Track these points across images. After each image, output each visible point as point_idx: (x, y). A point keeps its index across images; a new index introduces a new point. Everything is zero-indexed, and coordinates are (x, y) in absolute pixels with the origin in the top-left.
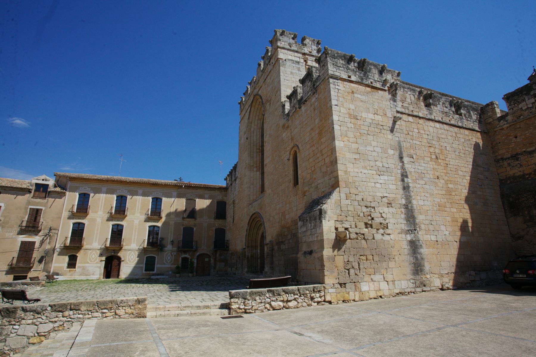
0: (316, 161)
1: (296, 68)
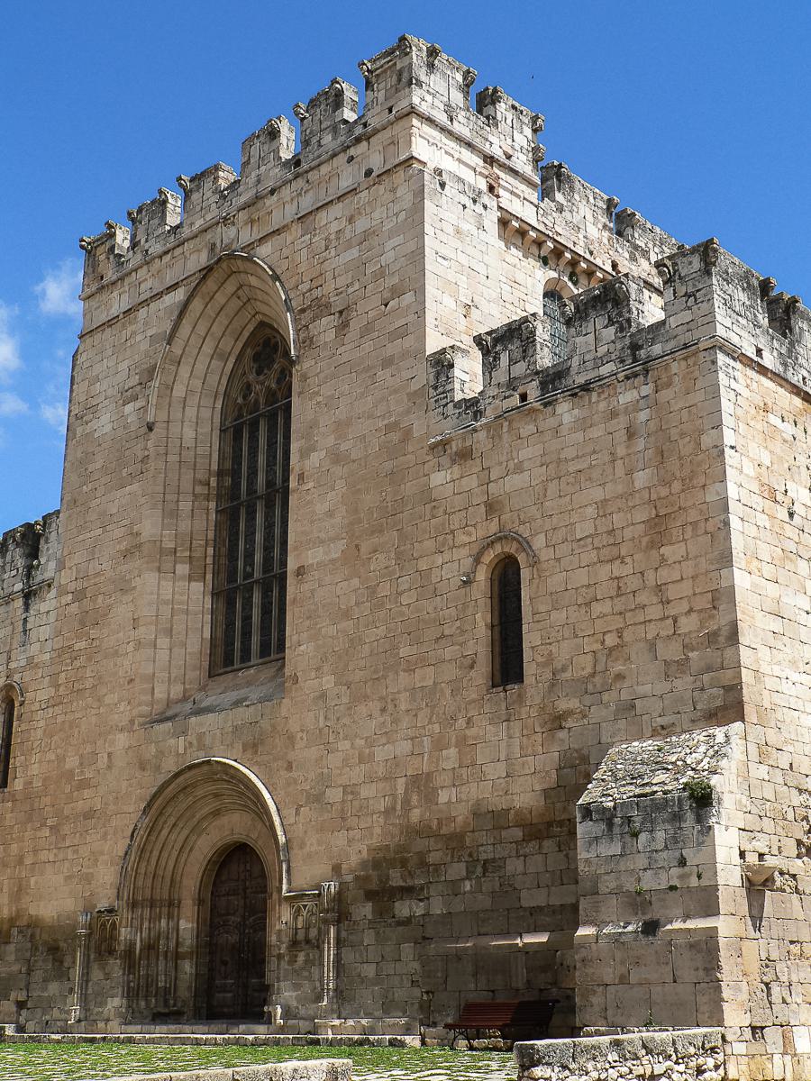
0: (628, 615)
1: (472, 213)
